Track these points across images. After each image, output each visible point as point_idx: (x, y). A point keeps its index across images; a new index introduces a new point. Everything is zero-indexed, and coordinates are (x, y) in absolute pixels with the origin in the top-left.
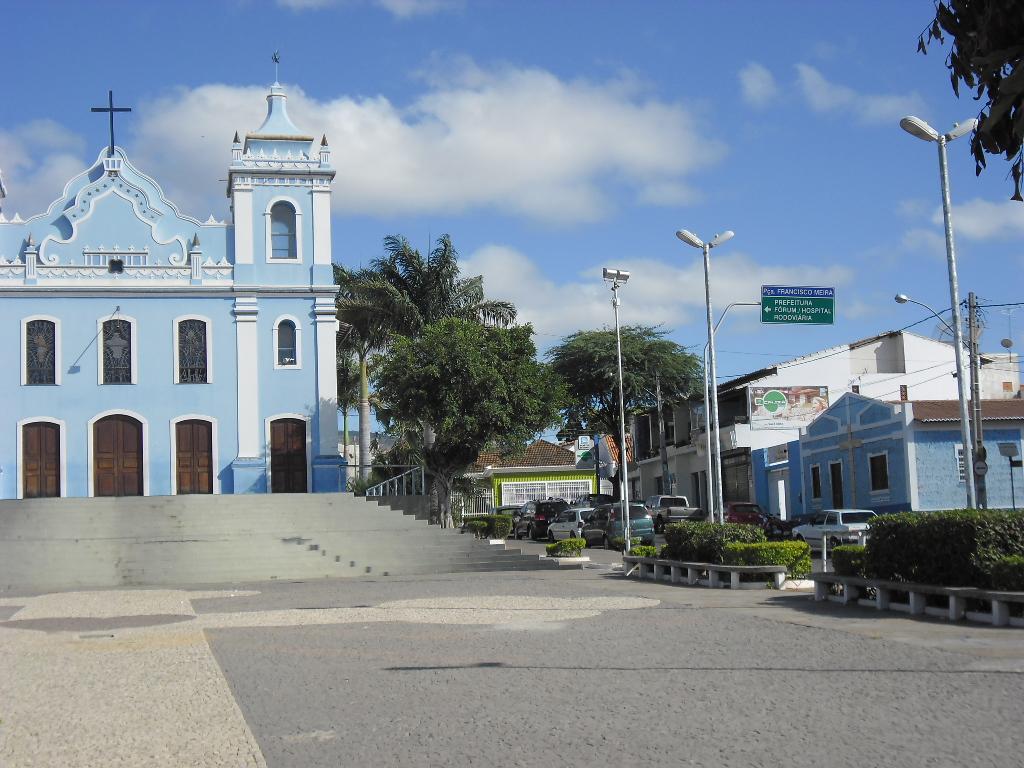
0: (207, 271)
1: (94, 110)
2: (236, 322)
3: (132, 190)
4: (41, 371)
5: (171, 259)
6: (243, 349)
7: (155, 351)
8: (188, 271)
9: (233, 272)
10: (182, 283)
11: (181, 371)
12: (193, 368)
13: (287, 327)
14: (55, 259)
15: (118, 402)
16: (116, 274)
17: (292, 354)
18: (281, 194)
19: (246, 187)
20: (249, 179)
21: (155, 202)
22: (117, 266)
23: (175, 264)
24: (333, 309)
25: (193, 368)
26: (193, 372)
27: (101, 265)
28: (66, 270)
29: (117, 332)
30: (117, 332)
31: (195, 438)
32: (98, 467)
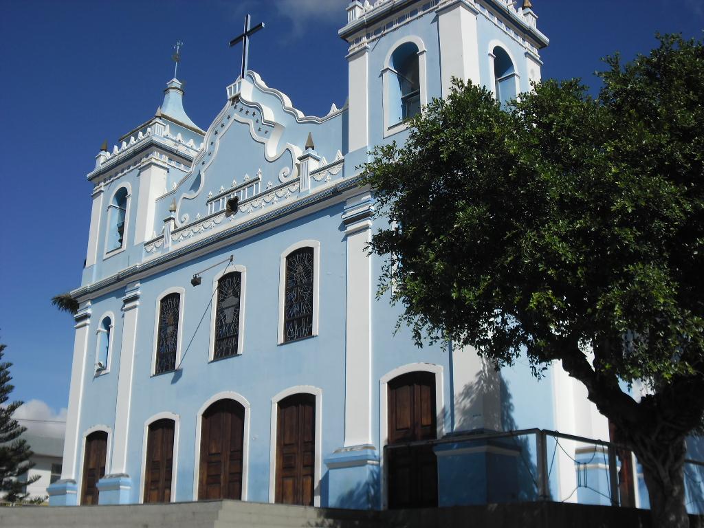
2: (345, 239)
3: (250, 109)
8: (297, 185)
9: (343, 167)
10: (288, 198)
11: (288, 323)
14: (187, 218)
18: (403, 36)
19: (363, 46)
20: (365, 39)
21: (269, 114)
22: (233, 206)
23: (285, 181)
26: (300, 325)
27: (221, 209)
28: (192, 228)
32: (208, 476)
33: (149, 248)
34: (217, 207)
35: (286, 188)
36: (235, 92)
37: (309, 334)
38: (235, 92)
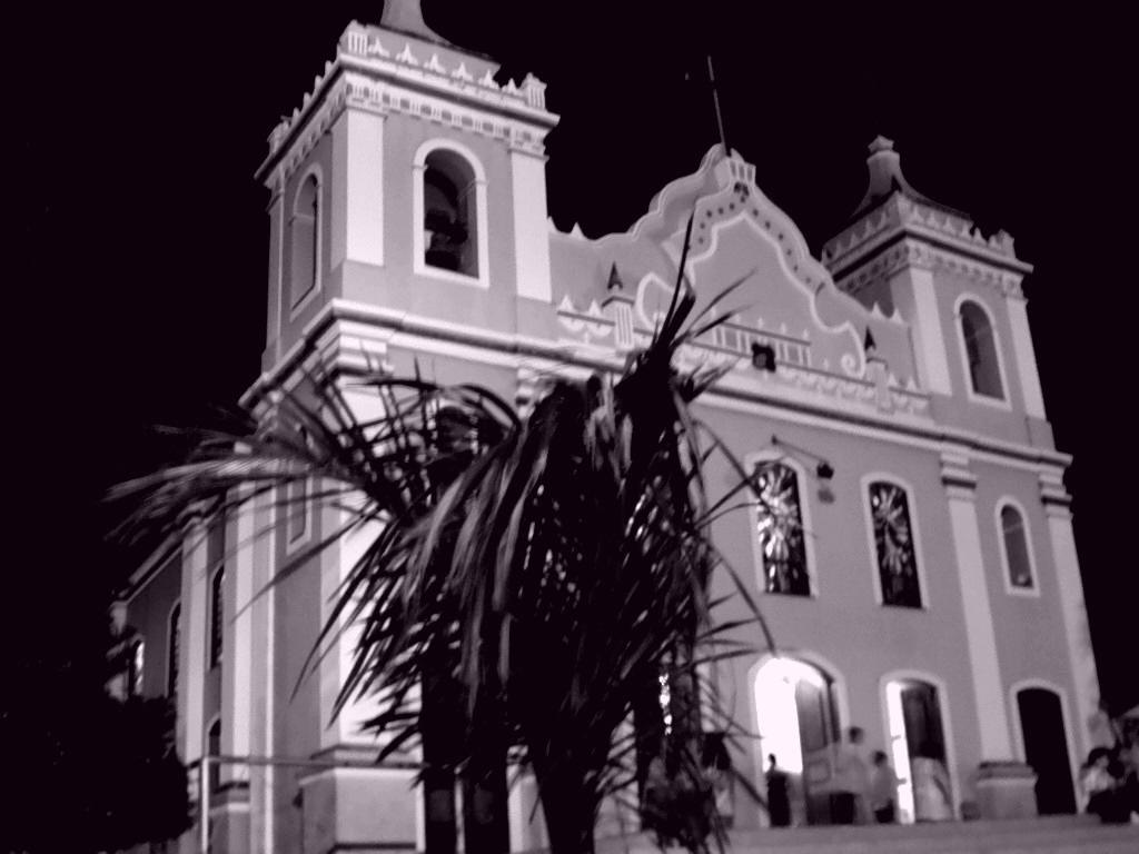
16: (765, 374)
22: (764, 357)
23: (850, 373)
24: (1061, 494)
35: (851, 388)
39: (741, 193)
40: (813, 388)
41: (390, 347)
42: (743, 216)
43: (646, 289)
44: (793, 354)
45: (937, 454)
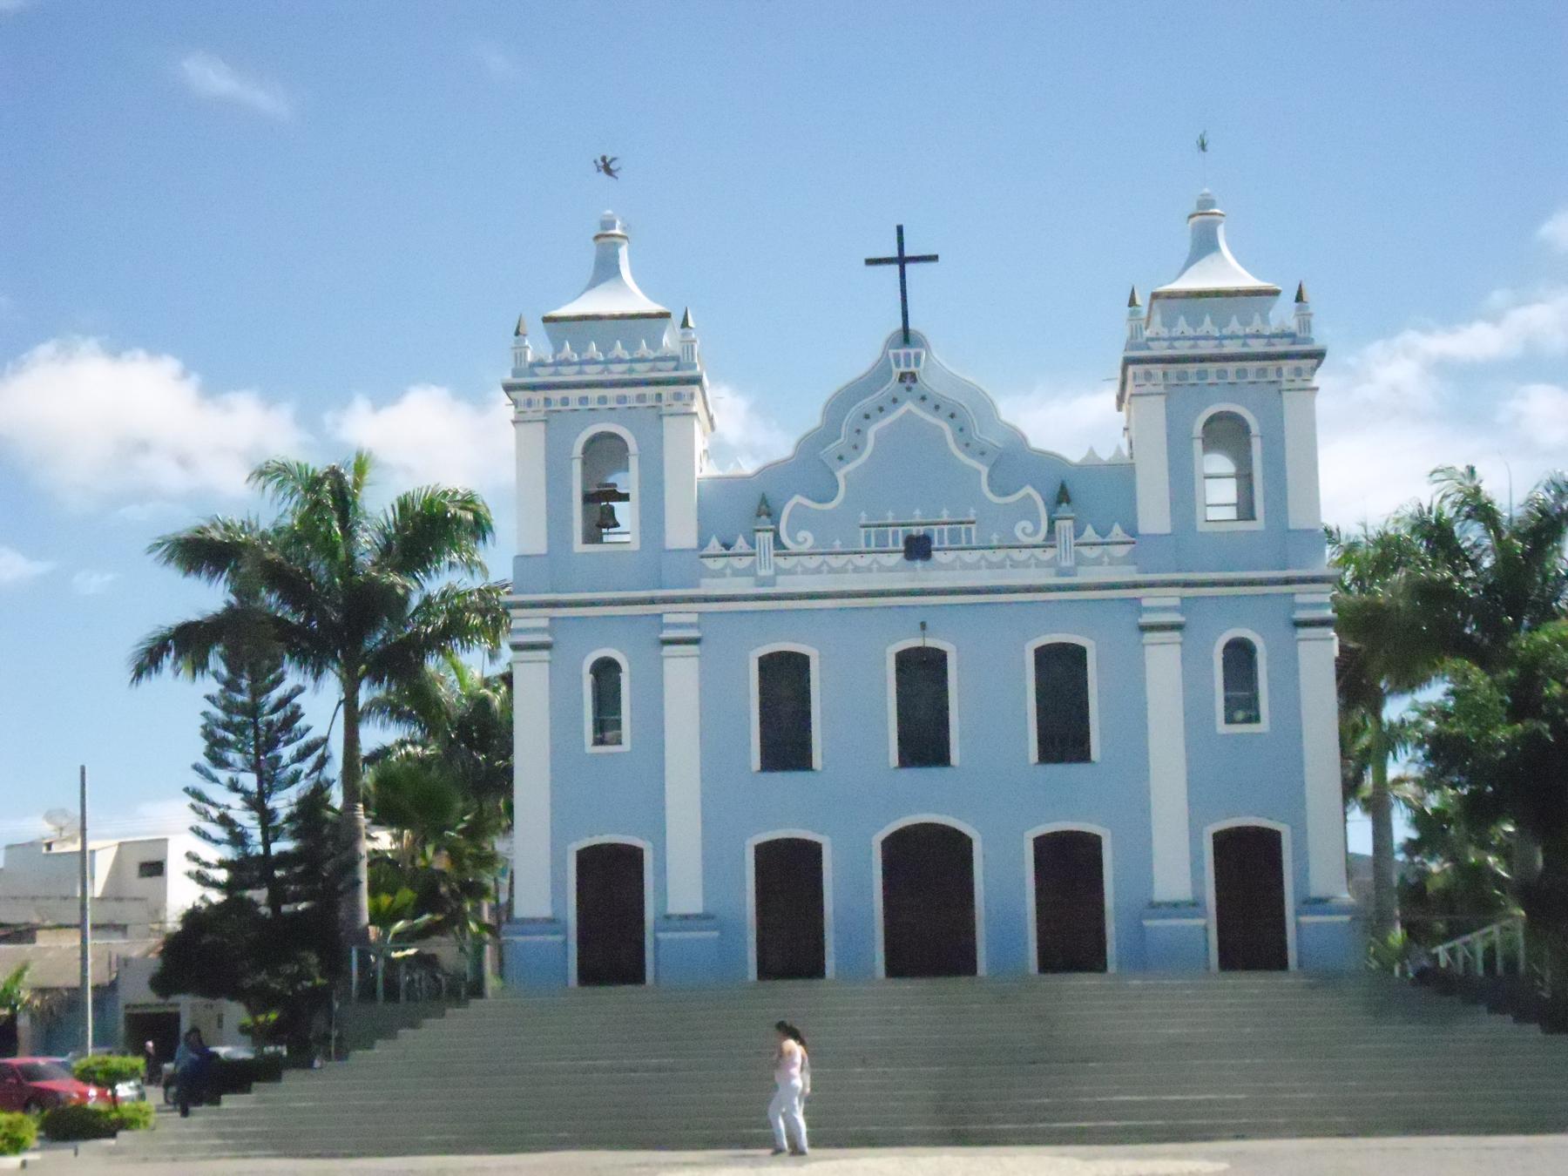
0: (1084, 550)
1: (870, 262)
4: (786, 743)
5: (1019, 534)
6: (1157, 698)
7: (992, 706)
8: (1049, 554)
12: (1064, 735)
13: (1240, 657)
14: (806, 539)
15: (926, 801)
16: (919, 564)
17: (1257, 709)
18: (1224, 400)
19: (1154, 389)
22: (918, 548)
25: (1064, 735)
27: (891, 547)
28: (827, 558)
29: (922, 673)
30: (922, 673)
31: (1069, 866)
33: (709, 563)
34: (881, 540)
36: (908, 365)
37: (1083, 756)
38: (908, 365)
39: (908, 383)
40: (975, 566)
41: (552, 619)
42: (909, 406)
43: (790, 516)
44: (955, 537)
45: (1138, 600)
